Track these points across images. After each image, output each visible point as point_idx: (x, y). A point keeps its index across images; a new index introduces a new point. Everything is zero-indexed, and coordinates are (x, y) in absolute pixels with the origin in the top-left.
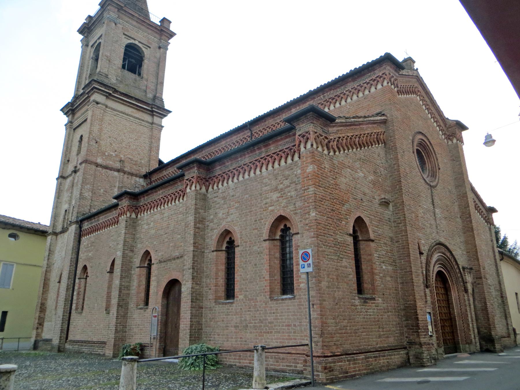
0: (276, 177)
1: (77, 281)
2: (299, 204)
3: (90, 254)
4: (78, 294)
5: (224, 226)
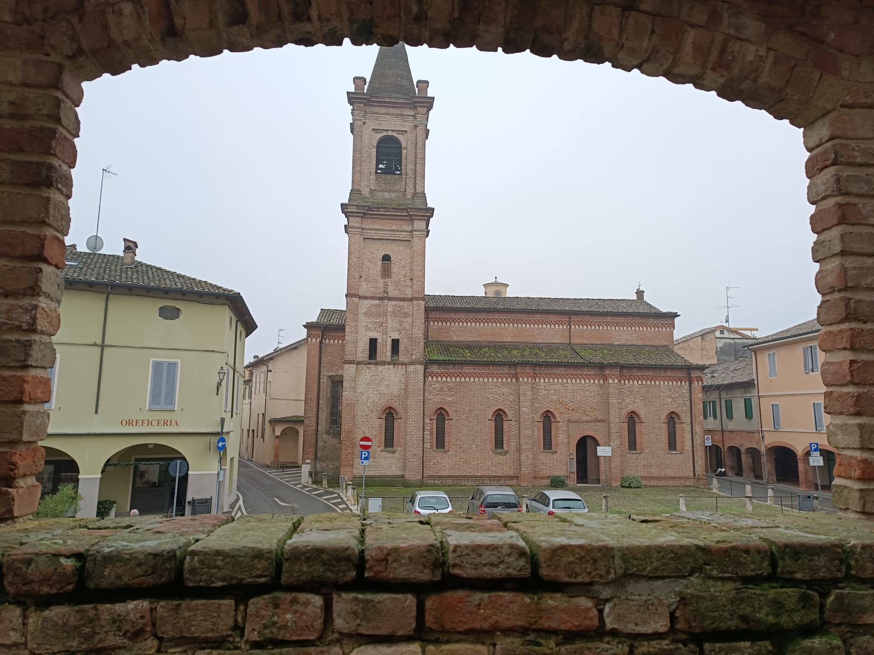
0: (670, 389)
1: (427, 421)
2: (684, 408)
3: (448, 399)
4: (431, 434)
5: (631, 408)
